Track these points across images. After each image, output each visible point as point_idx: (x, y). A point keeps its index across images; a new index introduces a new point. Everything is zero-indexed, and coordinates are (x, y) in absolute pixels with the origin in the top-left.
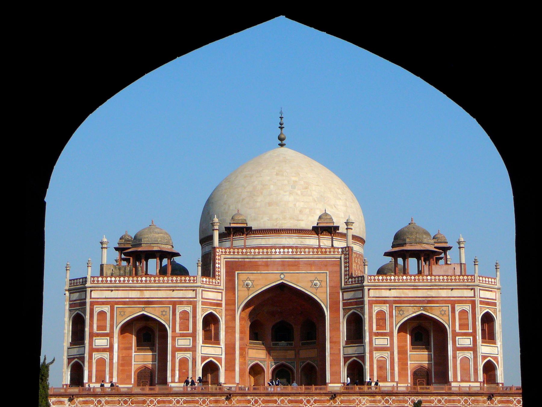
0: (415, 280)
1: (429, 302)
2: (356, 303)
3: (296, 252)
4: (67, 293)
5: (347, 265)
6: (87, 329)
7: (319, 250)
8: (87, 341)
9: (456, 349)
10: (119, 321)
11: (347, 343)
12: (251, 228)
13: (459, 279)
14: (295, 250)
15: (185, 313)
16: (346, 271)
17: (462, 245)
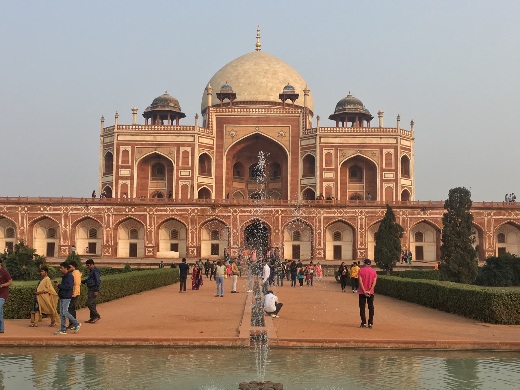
0: (354, 131)
1: (364, 147)
2: (310, 148)
3: (268, 112)
4: (102, 138)
5: (305, 120)
6: (114, 163)
7: (285, 110)
8: (114, 172)
9: (382, 181)
10: (137, 158)
11: (303, 176)
12: (234, 96)
13: (386, 131)
14: (266, 110)
15: (185, 152)
16: (303, 125)
17: (381, 115)
